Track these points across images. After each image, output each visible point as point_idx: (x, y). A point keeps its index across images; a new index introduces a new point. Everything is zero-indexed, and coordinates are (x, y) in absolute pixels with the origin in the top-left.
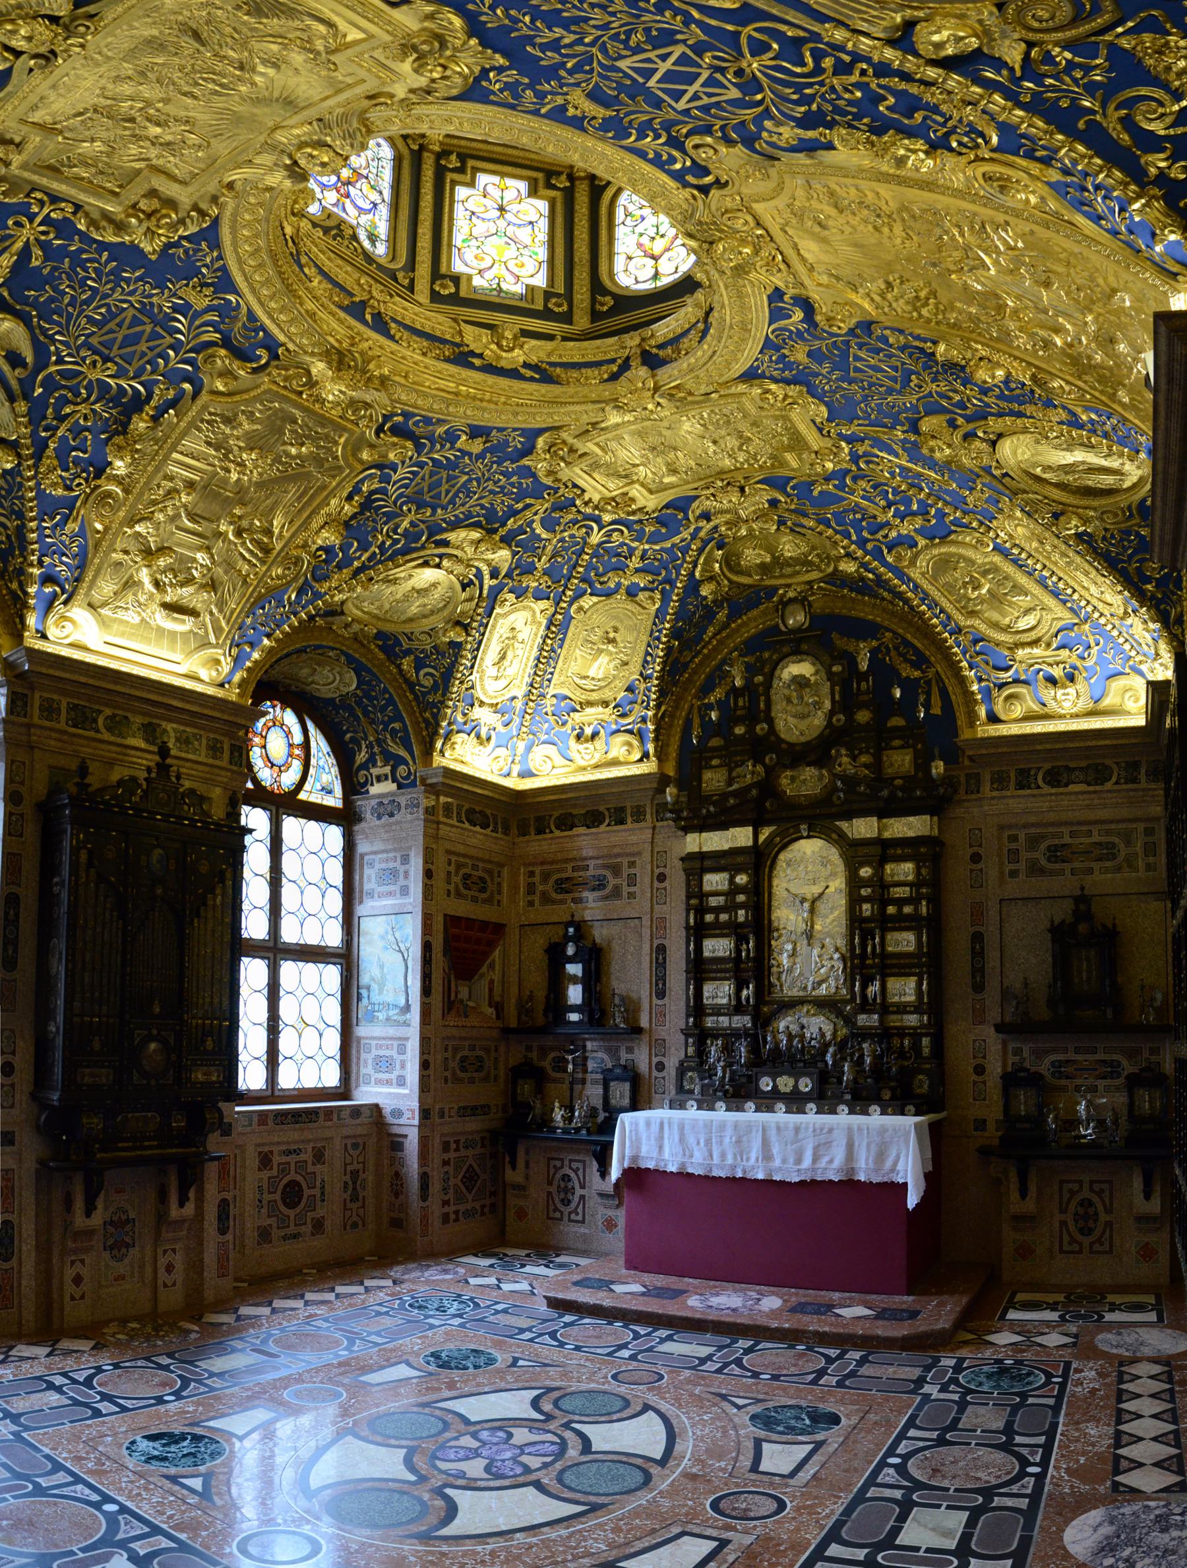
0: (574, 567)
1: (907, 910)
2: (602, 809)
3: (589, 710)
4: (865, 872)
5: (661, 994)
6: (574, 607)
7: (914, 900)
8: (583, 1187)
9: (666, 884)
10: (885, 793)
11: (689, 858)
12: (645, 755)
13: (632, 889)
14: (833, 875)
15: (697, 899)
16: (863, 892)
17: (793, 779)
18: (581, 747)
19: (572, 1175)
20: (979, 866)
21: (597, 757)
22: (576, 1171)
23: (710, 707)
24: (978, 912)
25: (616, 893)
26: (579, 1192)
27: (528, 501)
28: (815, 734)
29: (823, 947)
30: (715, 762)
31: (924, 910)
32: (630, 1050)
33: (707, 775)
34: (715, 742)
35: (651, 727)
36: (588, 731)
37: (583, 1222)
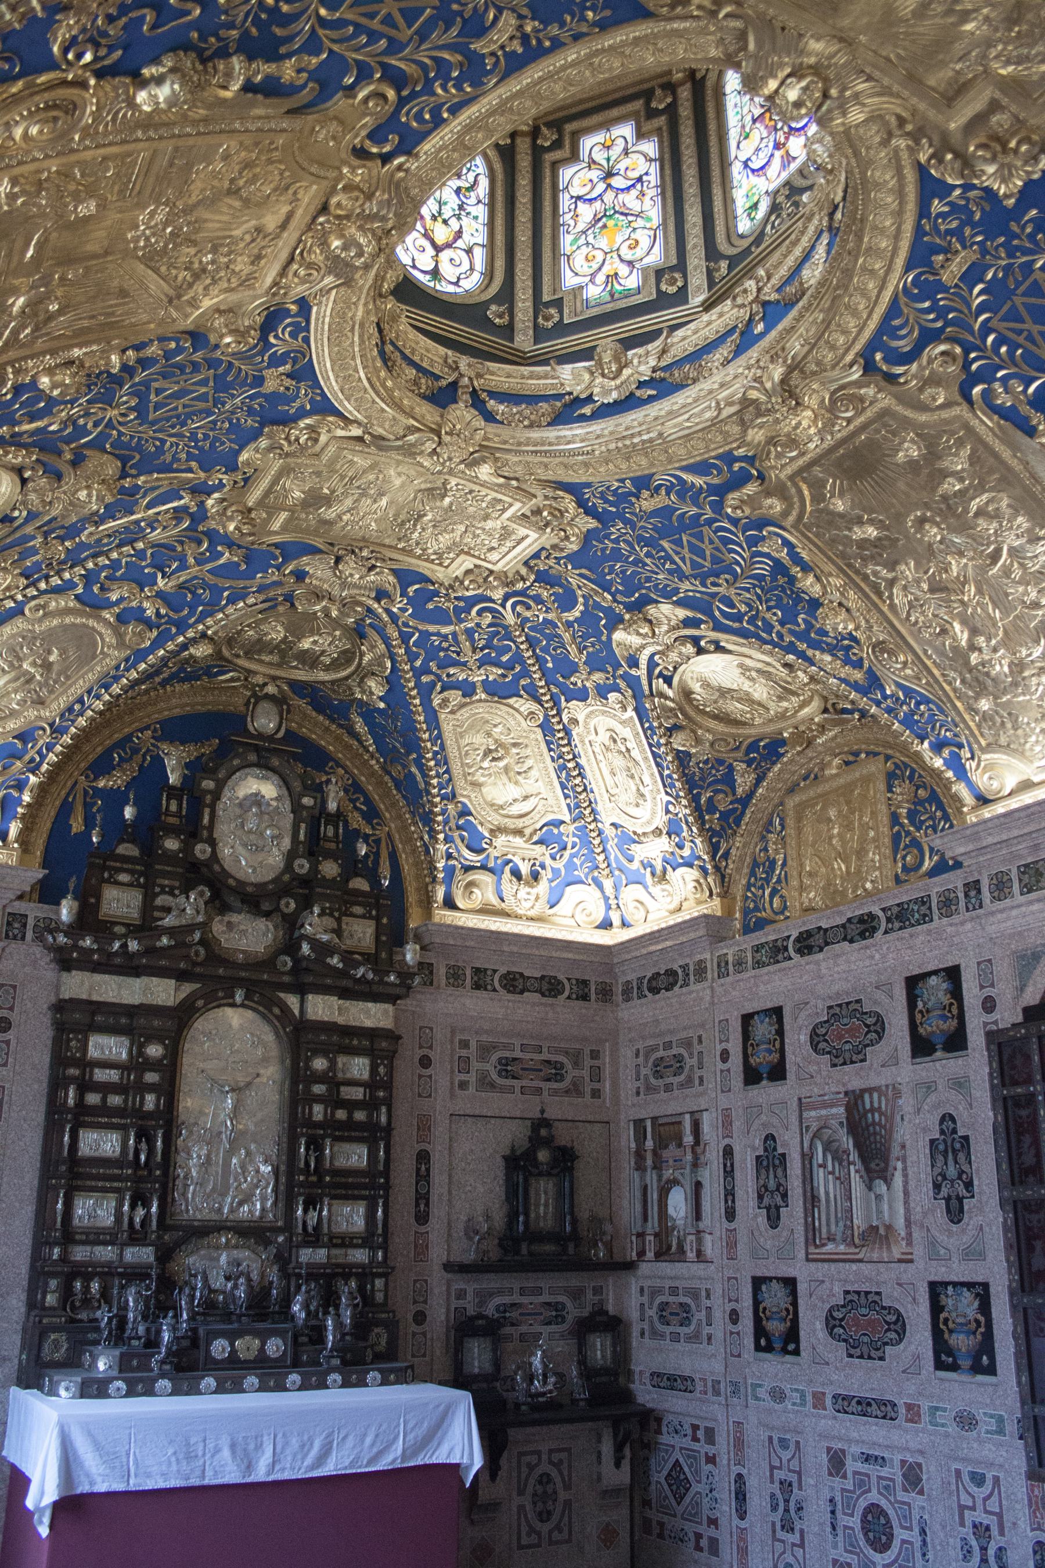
0: (95, 556)
1: (360, 1116)
4: (319, 1064)
6: (40, 601)
7: (371, 1105)
10: (361, 972)
11: (61, 1007)
14: (265, 1060)
15: (67, 1065)
16: (318, 1089)
17: (229, 924)
20: (427, 1072)
23: (115, 799)
24: (424, 1126)
27: (193, 464)
28: (271, 876)
29: (248, 1153)
30: (124, 878)
31: (383, 1119)
33: (110, 893)
34: (126, 849)
35: (26, 798)
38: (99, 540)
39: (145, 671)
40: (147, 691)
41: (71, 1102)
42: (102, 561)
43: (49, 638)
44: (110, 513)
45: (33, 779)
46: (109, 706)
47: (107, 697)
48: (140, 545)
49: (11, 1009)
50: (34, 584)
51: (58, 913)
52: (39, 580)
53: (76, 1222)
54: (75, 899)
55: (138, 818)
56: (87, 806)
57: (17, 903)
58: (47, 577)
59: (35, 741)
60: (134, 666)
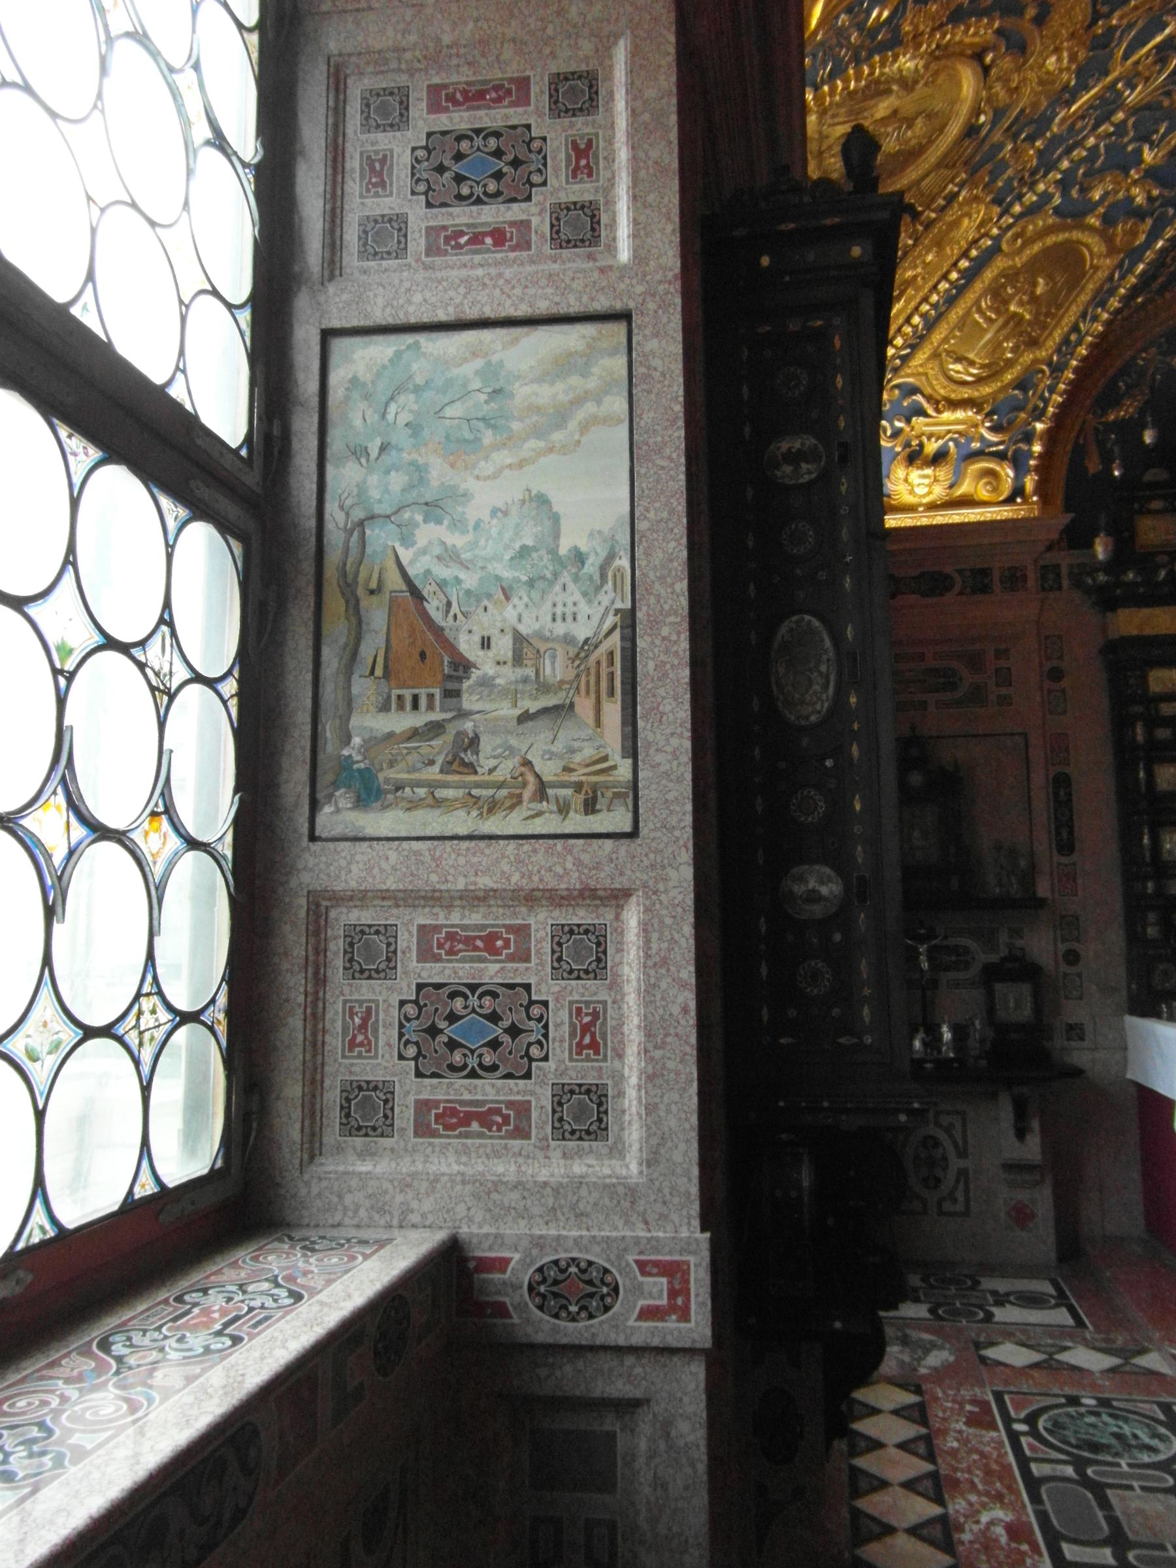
2: (948, 570)
3: (947, 416)
5: (1066, 847)
8: (963, 1154)
9: (1065, 683)
12: (1018, 491)
13: (1004, 691)
18: (915, 475)
19: (942, 1136)
21: (939, 492)
22: (948, 1130)
25: (977, 695)
26: (955, 1163)
30: (1156, 505)
32: (1016, 933)
35: (1037, 448)
36: (931, 447)
37: (967, 1213)
38: (1072, 127)
39: (1144, 272)
40: (1144, 304)
41: (1140, 738)
42: (1079, 153)
43: (1033, 268)
44: (1086, 74)
45: (1039, 426)
46: (1108, 324)
47: (1105, 316)
48: (1120, 115)
49: (1061, 658)
50: (1006, 211)
51: (1094, 556)
52: (1011, 204)
53: (1165, 856)
54: (1109, 534)
55: (1160, 439)
56: (1101, 444)
57: (1048, 555)
58: (1020, 197)
59: (1036, 386)
60: (1130, 270)
